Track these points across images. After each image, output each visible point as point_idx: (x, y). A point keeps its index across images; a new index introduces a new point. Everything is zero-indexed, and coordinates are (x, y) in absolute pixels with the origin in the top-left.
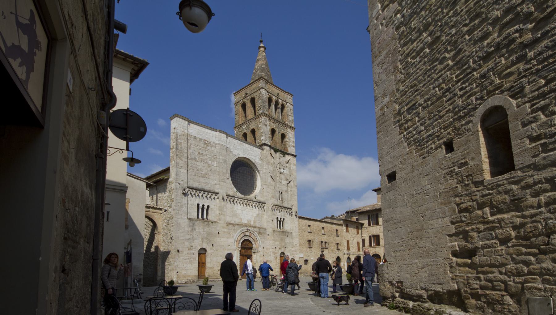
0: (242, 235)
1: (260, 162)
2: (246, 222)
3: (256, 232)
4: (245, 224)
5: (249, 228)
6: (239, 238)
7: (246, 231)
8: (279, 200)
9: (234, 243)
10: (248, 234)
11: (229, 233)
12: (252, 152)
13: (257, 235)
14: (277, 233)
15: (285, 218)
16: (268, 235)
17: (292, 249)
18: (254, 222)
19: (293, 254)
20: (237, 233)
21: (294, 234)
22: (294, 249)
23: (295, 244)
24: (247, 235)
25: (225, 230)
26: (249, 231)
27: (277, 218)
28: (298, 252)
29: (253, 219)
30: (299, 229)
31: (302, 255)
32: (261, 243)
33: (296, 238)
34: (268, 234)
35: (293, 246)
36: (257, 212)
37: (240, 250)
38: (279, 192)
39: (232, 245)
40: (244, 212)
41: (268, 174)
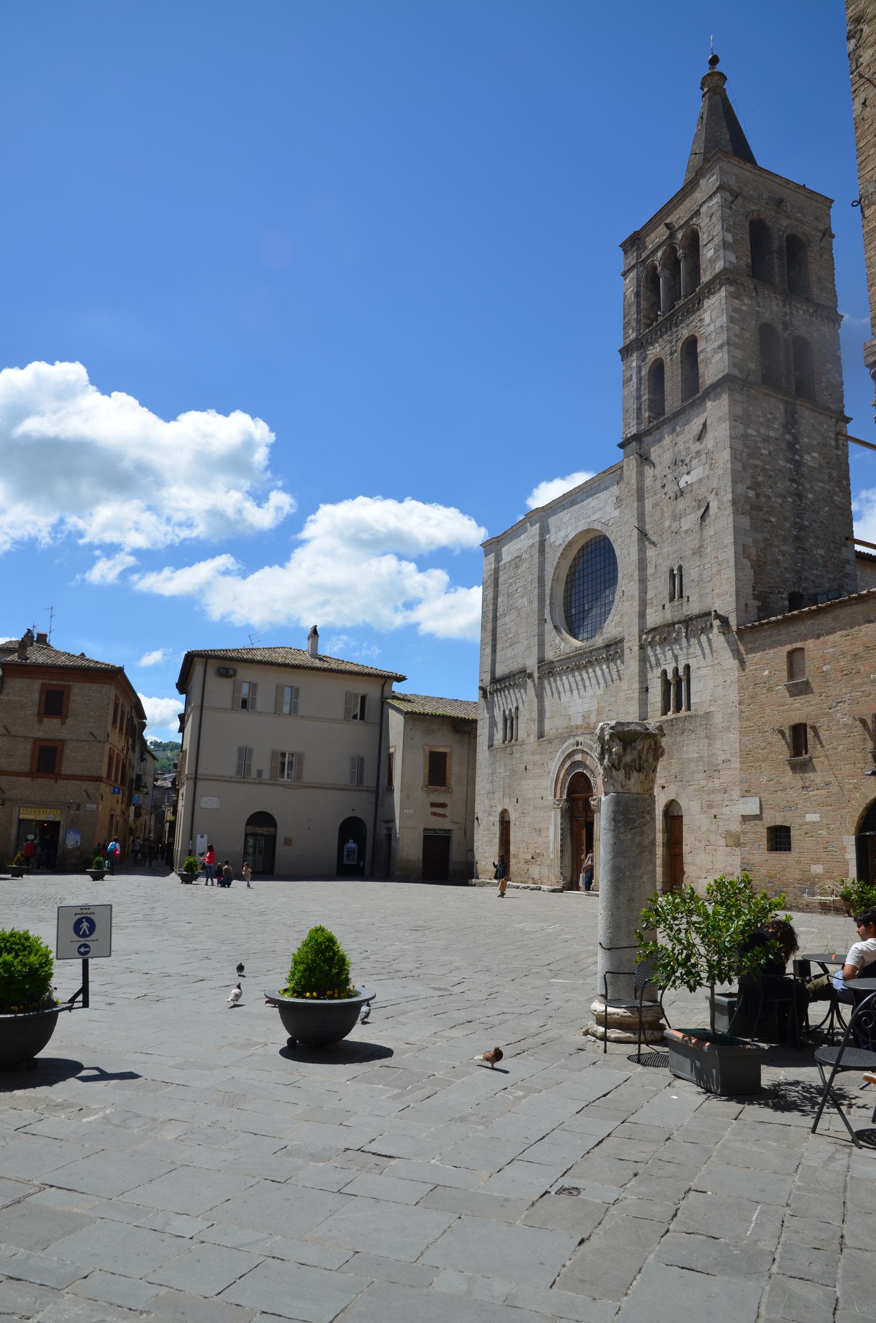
1: (616, 513)
2: (579, 722)
4: (577, 727)
5: (580, 739)
7: (571, 750)
8: (672, 599)
10: (578, 757)
15: (691, 662)
17: (711, 785)
18: (599, 712)
19: (710, 807)
21: (718, 719)
22: (717, 783)
23: (720, 759)
26: (580, 747)
27: (665, 672)
28: (736, 794)
29: (594, 706)
30: (741, 689)
31: (751, 807)
33: (728, 730)
35: (712, 771)
39: (547, 796)
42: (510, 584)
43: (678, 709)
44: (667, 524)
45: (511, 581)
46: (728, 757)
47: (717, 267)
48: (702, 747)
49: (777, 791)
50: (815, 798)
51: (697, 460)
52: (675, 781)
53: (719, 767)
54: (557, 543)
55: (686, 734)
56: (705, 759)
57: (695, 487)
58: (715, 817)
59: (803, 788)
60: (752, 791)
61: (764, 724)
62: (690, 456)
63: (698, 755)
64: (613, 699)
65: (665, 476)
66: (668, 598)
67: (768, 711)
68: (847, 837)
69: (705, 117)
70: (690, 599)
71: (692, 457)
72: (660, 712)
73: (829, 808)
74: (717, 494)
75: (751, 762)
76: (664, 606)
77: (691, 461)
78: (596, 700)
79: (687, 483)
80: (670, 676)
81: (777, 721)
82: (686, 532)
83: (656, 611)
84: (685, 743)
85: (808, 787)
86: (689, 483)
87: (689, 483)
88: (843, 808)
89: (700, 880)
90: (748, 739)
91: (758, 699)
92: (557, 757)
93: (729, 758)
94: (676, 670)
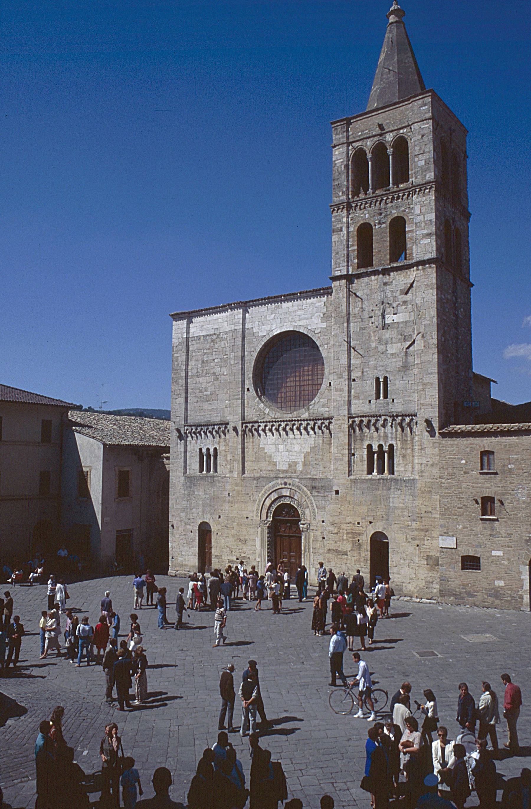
0: (274, 496)
1: (324, 325)
3: (305, 489)
6: (268, 503)
7: (280, 486)
8: (378, 397)
9: (257, 513)
11: (248, 494)
12: (299, 313)
13: (309, 492)
14: (365, 486)
16: (337, 492)
20: (263, 492)
24: (284, 494)
25: (240, 488)
26: (288, 486)
32: (316, 510)
34: (335, 488)
36: (313, 443)
37: (268, 525)
38: (378, 379)
40: (281, 447)
41: (340, 346)
42: (205, 354)
43: (381, 471)
44: (373, 345)
45: (205, 351)
46: (430, 509)
47: (428, 176)
48: (407, 500)
49: (470, 535)
50: (500, 542)
51: (404, 307)
52: (382, 520)
53: (422, 515)
54: (260, 334)
55: (392, 490)
56: (410, 509)
57: (401, 326)
58: (418, 546)
59: (490, 535)
60: (450, 533)
61: (462, 493)
62: (397, 303)
63: (403, 505)
64: (321, 457)
65: (372, 310)
66: (374, 396)
67: (464, 485)
68: (523, 566)
69: (395, 43)
70: (395, 401)
71: (399, 304)
72: (366, 472)
73: (510, 549)
74: (423, 336)
75: (449, 515)
76: (370, 402)
77: (397, 306)
78: (303, 455)
79: (393, 320)
80: (375, 448)
81: (472, 493)
82: (392, 354)
83: (363, 403)
84: (392, 496)
85: (495, 535)
86: (395, 321)
87: (395, 321)
88: (521, 550)
89: (404, 585)
90: (447, 500)
91: (456, 477)
92: (264, 490)
93: (431, 510)
94: (380, 446)
